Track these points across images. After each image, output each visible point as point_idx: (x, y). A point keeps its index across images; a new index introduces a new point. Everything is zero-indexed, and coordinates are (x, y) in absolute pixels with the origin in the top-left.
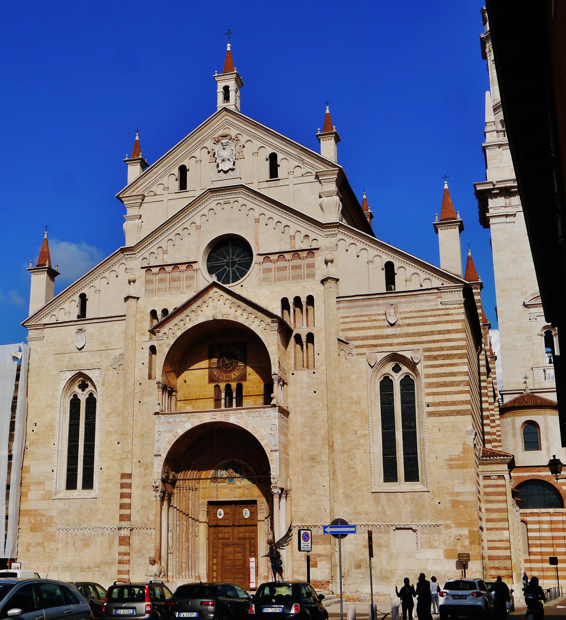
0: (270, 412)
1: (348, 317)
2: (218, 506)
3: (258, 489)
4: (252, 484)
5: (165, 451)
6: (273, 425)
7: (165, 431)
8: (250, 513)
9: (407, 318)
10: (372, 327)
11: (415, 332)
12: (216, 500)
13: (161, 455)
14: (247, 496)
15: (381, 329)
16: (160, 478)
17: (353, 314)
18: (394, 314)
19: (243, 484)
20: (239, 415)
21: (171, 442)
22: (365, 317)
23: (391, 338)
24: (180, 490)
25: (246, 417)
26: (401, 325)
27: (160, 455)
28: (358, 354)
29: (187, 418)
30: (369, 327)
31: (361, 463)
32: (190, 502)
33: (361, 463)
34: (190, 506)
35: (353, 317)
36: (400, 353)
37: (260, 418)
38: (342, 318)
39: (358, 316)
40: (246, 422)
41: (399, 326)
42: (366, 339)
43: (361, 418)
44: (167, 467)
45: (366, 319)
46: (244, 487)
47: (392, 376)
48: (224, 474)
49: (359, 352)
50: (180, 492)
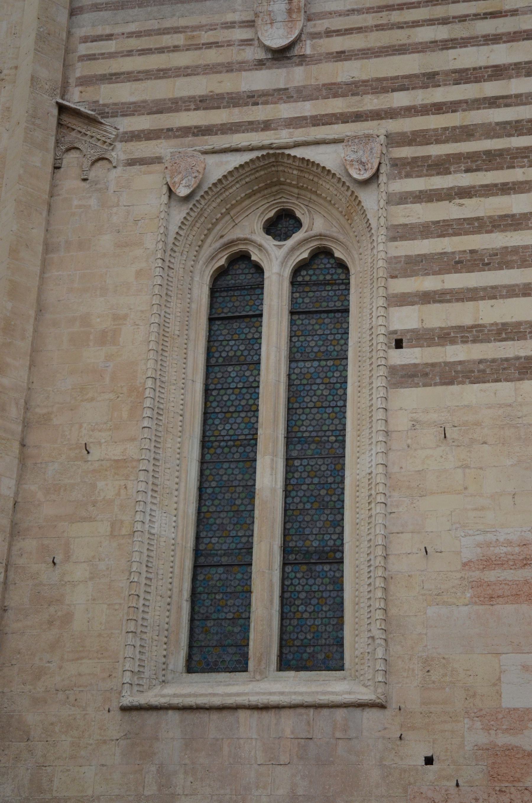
1: (109, 37)
9: (339, 33)
10: (197, 67)
11: (364, 77)
15: (230, 75)
17: (133, 27)
18: (285, 16)
22: (175, 36)
23: (266, 103)
26: (311, 56)
28: (132, 163)
30: (187, 67)
31: (91, 579)
33: (91, 579)
35: (130, 35)
36: (298, 152)
38: (85, 40)
39: (148, 33)
41: (303, 59)
42: (170, 110)
43: (112, 396)
45: (176, 43)
47: (260, 247)
49: (137, 155)
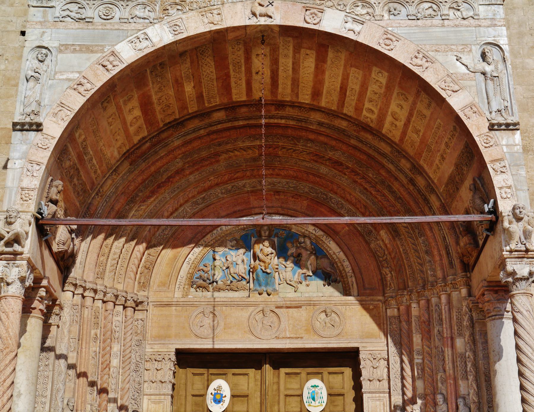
0: (476, 5)
2: (212, 371)
3: (364, 313)
4: (337, 294)
5: (62, 114)
6: (488, 48)
7: (64, 48)
8: (330, 395)
12: (210, 346)
13: (45, 127)
14: (322, 333)
16: (32, 208)
19: (307, 295)
20: (359, 8)
21: (88, 86)
24: (84, 297)
25: (386, 16)
27: (38, 127)
29: (157, 8)
32: (116, 348)
34: (115, 362)
37: (437, 21)
40: (386, 33)
44: (61, 183)
46: (311, 303)
48: (239, 262)
50: (83, 306)
